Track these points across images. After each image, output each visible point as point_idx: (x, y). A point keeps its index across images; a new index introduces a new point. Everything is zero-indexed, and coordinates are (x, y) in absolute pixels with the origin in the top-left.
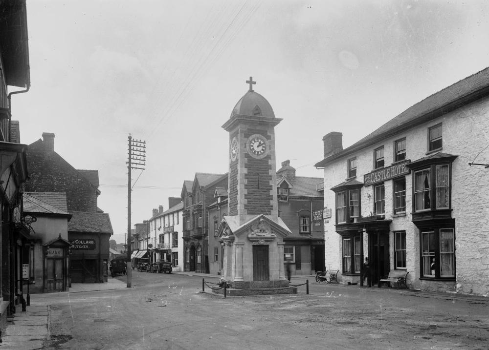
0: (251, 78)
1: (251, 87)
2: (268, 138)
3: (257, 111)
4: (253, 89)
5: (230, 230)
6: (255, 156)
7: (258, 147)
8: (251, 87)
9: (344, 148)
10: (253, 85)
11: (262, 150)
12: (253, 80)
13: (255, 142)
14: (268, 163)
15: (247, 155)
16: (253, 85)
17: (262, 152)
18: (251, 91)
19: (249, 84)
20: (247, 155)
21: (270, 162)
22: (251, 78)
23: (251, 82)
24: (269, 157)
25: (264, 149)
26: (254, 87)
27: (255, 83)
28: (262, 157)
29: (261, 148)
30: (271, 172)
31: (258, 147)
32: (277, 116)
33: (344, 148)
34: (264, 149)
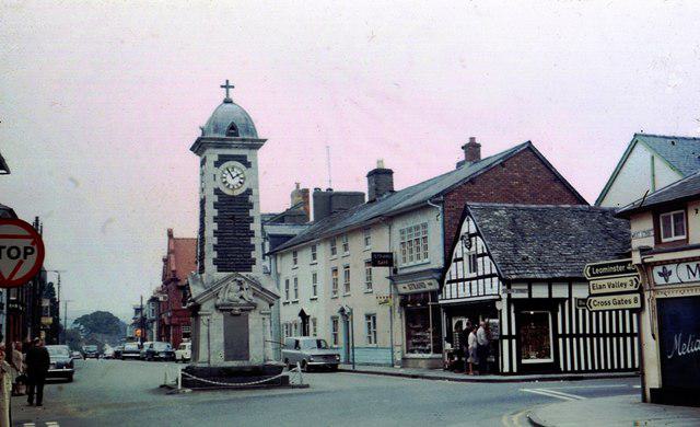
2: (248, 165)
9: (484, 154)
12: (230, 84)
15: (217, 191)
18: (228, 101)
19: (224, 89)
20: (217, 191)
21: (251, 198)
23: (227, 86)
24: (249, 192)
26: (233, 94)
28: (237, 193)
29: (237, 180)
30: (252, 213)
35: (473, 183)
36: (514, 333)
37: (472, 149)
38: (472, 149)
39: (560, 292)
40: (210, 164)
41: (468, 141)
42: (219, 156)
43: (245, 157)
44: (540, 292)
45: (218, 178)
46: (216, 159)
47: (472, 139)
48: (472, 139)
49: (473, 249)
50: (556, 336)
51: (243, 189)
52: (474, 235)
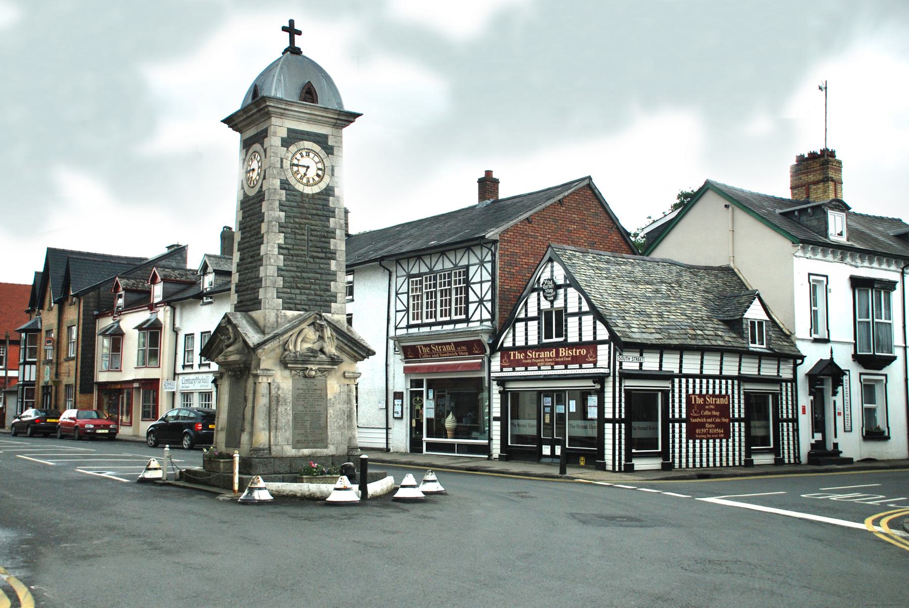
0: (292, 22)
1: (292, 40)
2: (329, 150)
3: (309, 94)
4: (297, 45)
5: (245, 342)
6: (300, 187)
7: (308, 167)
8: (292, 40)
9: (502, 196)
10: (296, 36)
11: (318, 175)
13: (302, 156)
14: (327, 205)
16: (296, 36)
17: (317, 179)
18: (293, 50)
22: (292, 22)
23: (291, 30)
24: (329, 191)
25: (320, 173)
26: (299, 41)
27: (299, 33)
28: (316, 190)
31: (308, 167)
32: (348, 107)
33: (502, 196)
34: (320, 173)
35: (530, 223)
36: (623, 416)
37: (488, 184)
38: (488, 184)
39: (671, 364)
40: (274, 141)
41: (483, 175)
42: (289, 130)
43: (326, 137)
44: (651, 363)
45: (286, 164)
46: (285, 135)
47: (489, 173)
48: (489, 173)
49: (559, 304)
50: (666, 421)
51: (323, 185)
52: (565, 286)
